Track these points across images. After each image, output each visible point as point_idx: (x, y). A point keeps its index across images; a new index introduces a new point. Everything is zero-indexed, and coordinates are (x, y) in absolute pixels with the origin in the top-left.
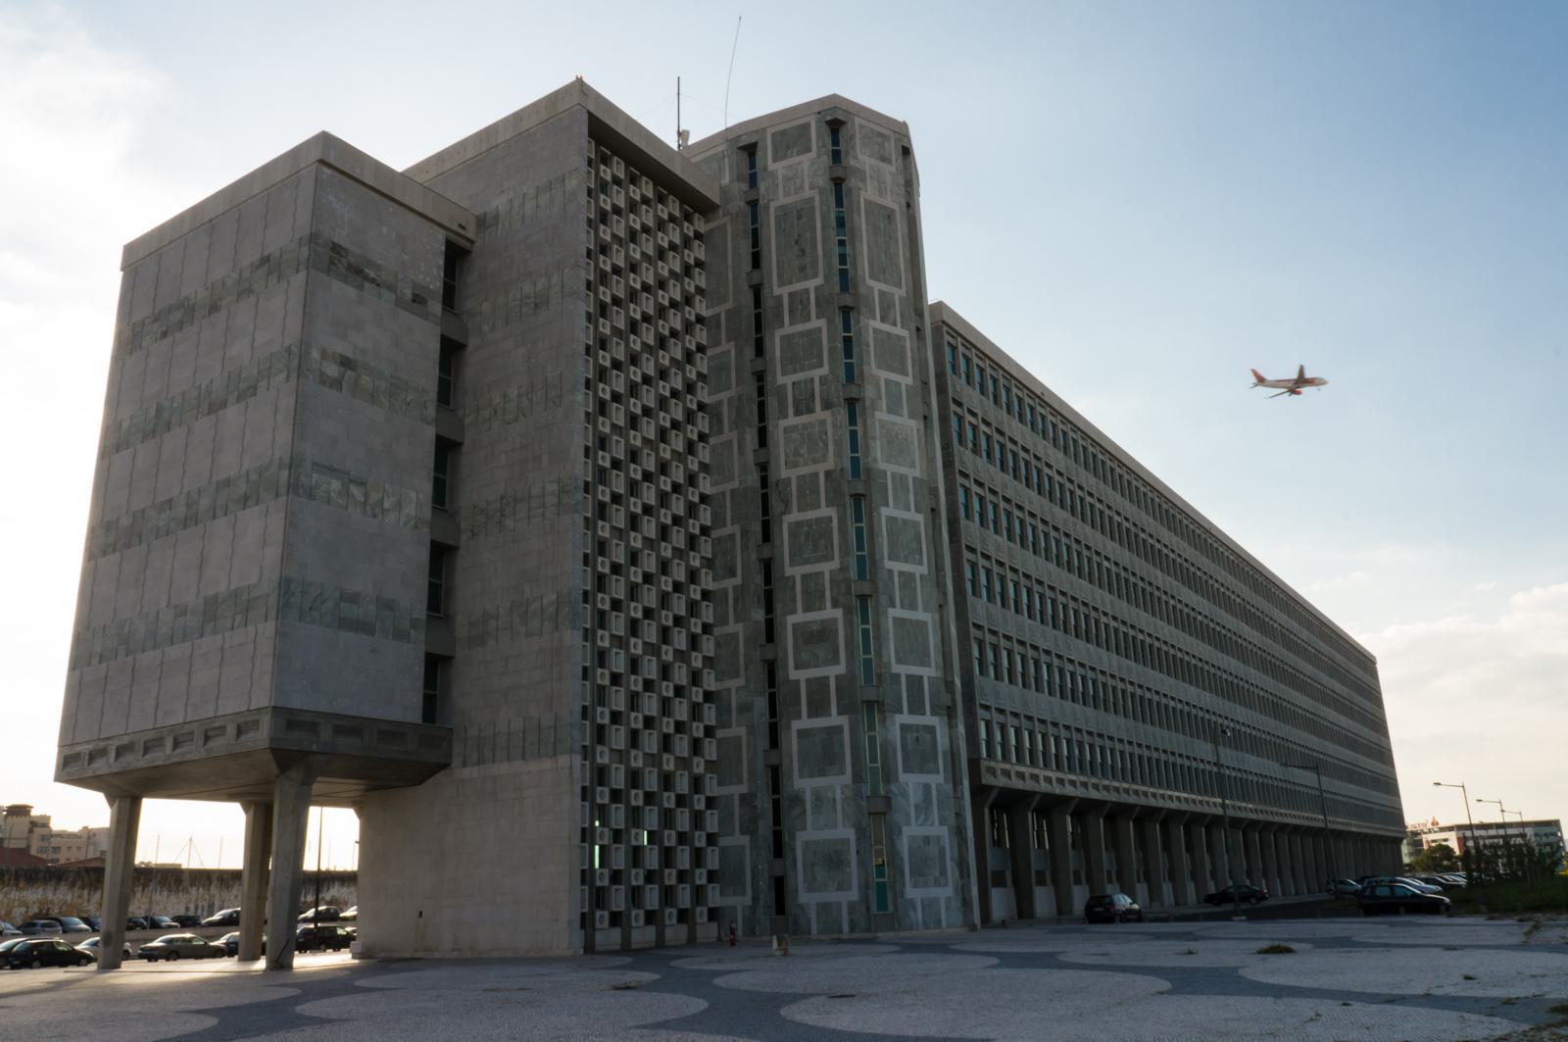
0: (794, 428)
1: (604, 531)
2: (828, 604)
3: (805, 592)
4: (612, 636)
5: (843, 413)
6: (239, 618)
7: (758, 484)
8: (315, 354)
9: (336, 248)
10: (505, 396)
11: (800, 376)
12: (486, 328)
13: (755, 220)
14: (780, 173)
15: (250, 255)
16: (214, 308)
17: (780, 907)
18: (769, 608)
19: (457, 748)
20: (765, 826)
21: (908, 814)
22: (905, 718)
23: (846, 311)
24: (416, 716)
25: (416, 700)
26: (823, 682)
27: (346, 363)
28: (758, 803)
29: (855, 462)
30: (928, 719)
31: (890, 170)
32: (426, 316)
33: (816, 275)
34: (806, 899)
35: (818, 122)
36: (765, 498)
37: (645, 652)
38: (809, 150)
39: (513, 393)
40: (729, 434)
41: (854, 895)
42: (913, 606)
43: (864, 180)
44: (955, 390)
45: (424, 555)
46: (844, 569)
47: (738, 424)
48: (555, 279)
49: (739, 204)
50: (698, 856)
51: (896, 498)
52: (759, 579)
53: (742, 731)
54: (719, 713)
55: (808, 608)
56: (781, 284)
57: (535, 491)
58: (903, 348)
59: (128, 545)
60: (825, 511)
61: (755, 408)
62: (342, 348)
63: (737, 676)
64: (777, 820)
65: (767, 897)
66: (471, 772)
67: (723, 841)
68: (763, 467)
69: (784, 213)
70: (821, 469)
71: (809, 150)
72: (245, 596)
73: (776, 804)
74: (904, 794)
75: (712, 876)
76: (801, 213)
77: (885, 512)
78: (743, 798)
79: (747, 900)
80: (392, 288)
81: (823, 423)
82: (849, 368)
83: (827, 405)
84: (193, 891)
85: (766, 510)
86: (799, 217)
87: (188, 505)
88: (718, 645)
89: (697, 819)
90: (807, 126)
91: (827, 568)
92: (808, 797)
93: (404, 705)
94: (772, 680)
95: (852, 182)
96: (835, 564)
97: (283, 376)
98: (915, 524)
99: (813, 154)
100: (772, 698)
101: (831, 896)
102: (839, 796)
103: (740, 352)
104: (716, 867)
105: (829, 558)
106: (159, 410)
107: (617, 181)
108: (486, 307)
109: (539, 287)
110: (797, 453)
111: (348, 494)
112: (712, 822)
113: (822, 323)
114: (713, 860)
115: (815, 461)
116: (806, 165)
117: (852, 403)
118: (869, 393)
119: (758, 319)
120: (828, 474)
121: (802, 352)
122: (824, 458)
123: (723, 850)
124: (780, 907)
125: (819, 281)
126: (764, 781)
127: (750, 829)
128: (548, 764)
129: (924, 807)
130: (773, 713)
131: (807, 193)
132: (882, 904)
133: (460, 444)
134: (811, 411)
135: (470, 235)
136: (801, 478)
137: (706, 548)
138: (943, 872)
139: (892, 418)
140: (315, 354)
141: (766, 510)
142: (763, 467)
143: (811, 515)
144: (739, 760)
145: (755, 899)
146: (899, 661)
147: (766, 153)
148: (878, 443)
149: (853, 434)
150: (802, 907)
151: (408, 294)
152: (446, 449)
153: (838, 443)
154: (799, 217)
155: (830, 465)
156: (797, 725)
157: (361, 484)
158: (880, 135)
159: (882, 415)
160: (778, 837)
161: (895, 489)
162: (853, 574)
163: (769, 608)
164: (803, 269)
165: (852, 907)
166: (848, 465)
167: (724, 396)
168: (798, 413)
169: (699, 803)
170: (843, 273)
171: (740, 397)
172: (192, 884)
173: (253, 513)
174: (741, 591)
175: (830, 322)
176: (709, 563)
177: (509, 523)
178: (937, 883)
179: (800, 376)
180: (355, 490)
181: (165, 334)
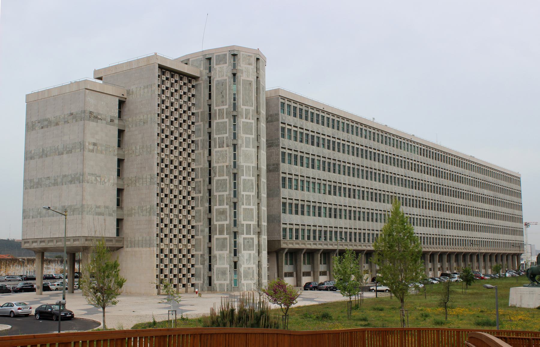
0: (218, 151)
1: (163, 185)
2: (225, 204)
3: (220, 200)
4: (165, 214)
5: (232, 148)
6: (72, 213)
7: (208, 166)
8: (87, 144)
9: (91, 113)
10: (136, 148)
11: (220, 136)
12: (130, 126)
13: (210, 83)
14: (218, 69)
15: (67, 112)
16: (57, 124)
17: (210, 284)
18: (210, 203)
19: (125, 243)
20: (207, 263)
21: (244, 262)
22: (245, 236)
23: (234, 116)
24: (115, 235)
25: (115, 231)
26: (223, 225)
27: (95, 144)
28: (205, 257)
29: (235, 163)
30: (252, 236)
31: (252, 68)
32: (114, 125)
33: (226, 105)
34: (216, 282)
35: (229, 54)
36: (210, 170)
37: (174, 217)
38: (226, 63)
39: (138, 148)
40: (200, 151)
41: (228, 282)
42: (249, 204)
43: (242, 73)
44: (282, 118)
45: (115, 192)
46: (230, 194)
47: (203, 148)
48: (149, 116)
49: (205, 77)
50: (189, 270)
51: (246, 173)
52: (207, 194)
53: (201, 237)
54: (196, 232)
55: (220, 205)
56: (216, 106)
57: (144, 177)
58: (252, 126)
59: (37, 187)
60: (225, 177)
61: (208, 143)
62: (94, 141)
63: (201, 222)
64: (210, 261)
65: (207, 281)
66: (128, 249)
67: (196, 266)
68: (210, 162)
69: (218, 83)
70: (225, 165)
71: (226, 63)
72: (73, 208)
73: (210, 257)
74: (243, 256)
75: (193, 275)
76: (222, 83)
77: (242, 178)
78: (202, 255)
79: (202, 282)
80: (105, 120)
81: (226, 151)
82: (235, 134)
83: (228, 146)
84: (28, 266)
85: (210, 174)
86: (222, 85)
87: (55, 180)
88: (196, 212)
89: (189, 260)
90: (225, 55)
91: (225, 194)
92: (218, 256)
93: (112, 232)
94: (210, 224)
95: (238, 75)
96: (227, 193)
97: (79, 150)
98: (252, 180)
99: (227, 65)
100: (210, 228)
101: (222, 282)
102: (225, 256)
103: (204, 126)
104: (194, 273)
105: (226, 191)
106: (43, 151)
107: (167, 79)
108: (130, 119)
109: (145, 117)
110: (219, 159)
111: (96, 180)
112: (193, 261)
113: (227, 120)
114: (193, 271)
115: (223, 162)
116: (225, 68)
117: (235, 146)
118: (240, 142)
119: (210, 114)
120: (227, 166)
121: (222, 128)
122: (226, 162)
123: (196, 268)
124: (210, 284)
125: (227, 107)
126: (207, 251)
127: (203, 264)
128: (148, 249)
129: (249, 260)
130: (210, 232)
131: (225, 78)
132: (235, 284)
133: (124, 160)
134: (223, 147)
135: (125, 97)
136: (219, 167)
137: (193, 184)
138: (253, 277)
139: (247, 149)
140: (87, 144)
141: (210, 174)
142: (210, 162)
143: (222, 178)
144: (201, 245)
145: (204, 282)
146: (244, 220)
147: (214, 61)
149: (235, 155)
150: (215, 284)
151: (109, 120)
152: (120, 162)
153: (230, 158)
154: (222, 85)
155: (227, 164)
156: (216, 237)
157: (100, 176)
158: (249, 56)
159: (244, 148)
160: (210, 266)
162: (232, 196)
163: (210, 203)
164: (223, 102)
165: (227, 284)
166: (232, 164)
167: (200, 138)
168: (219, 147)
169: (189, 256)
170: (234, 104)
171: (204, 140)
172: (28, 263)
173: (72, 186)
174: (202, 197)
175: (229, 120)
176: (194, 189)
177: (138, 184)
178: (251, 279)
179: (220, 136)
180: (98, 179)
181: (42, 128)
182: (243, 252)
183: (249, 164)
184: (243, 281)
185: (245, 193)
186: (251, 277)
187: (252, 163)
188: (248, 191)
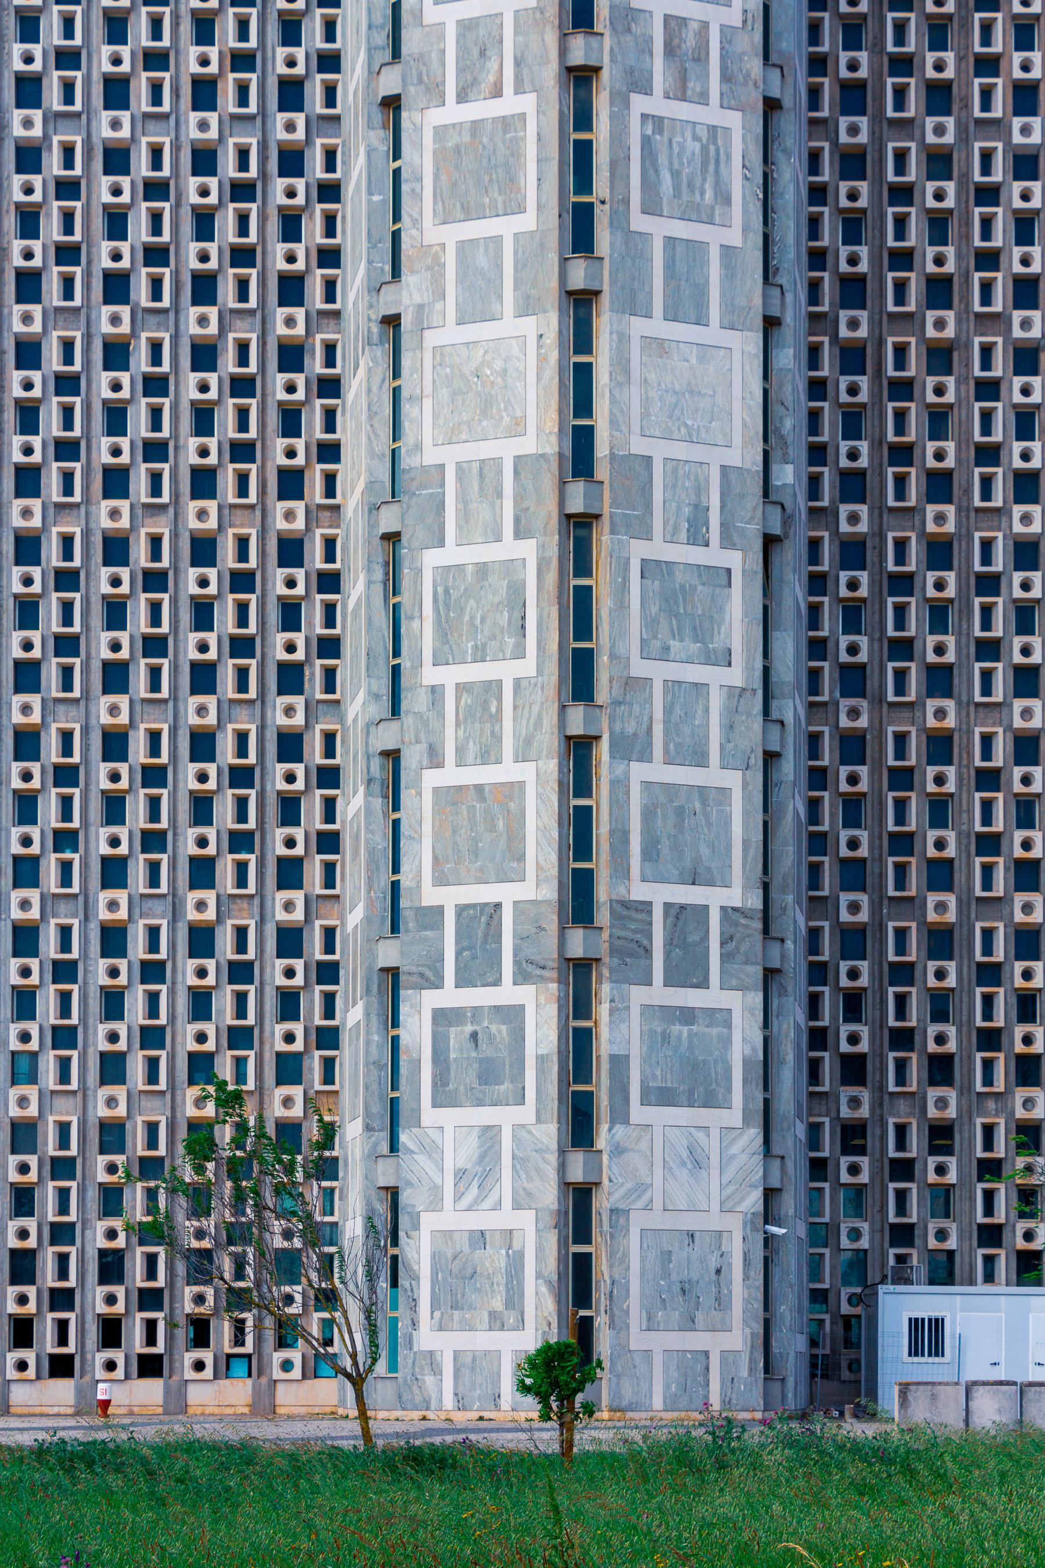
21: (437, 1191)
22: (450, 995)
30: (508, 993)
42: (489, 755)
51: (465, 516)
58: (516, 151)
74: (433, 1151)
129: (482, 1171)
138: (514, 1299)
146: (441, 880)
148: (427, 404)
161: (463, 500)
178: (496, 1322)
182: (430, 1115)
183: (486, 450)
184: (427, 1337)
185: (449, 676)
186: (498, 1304)
187: (517, 428)
188: (480, 656)
